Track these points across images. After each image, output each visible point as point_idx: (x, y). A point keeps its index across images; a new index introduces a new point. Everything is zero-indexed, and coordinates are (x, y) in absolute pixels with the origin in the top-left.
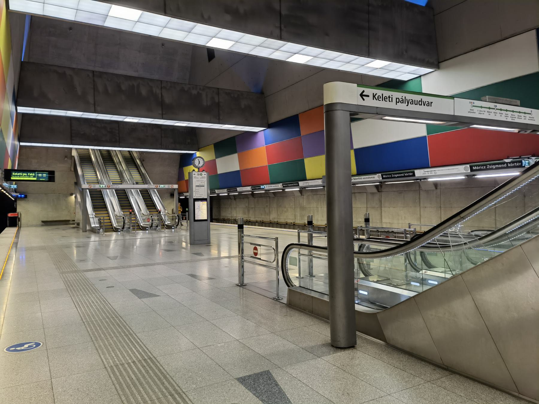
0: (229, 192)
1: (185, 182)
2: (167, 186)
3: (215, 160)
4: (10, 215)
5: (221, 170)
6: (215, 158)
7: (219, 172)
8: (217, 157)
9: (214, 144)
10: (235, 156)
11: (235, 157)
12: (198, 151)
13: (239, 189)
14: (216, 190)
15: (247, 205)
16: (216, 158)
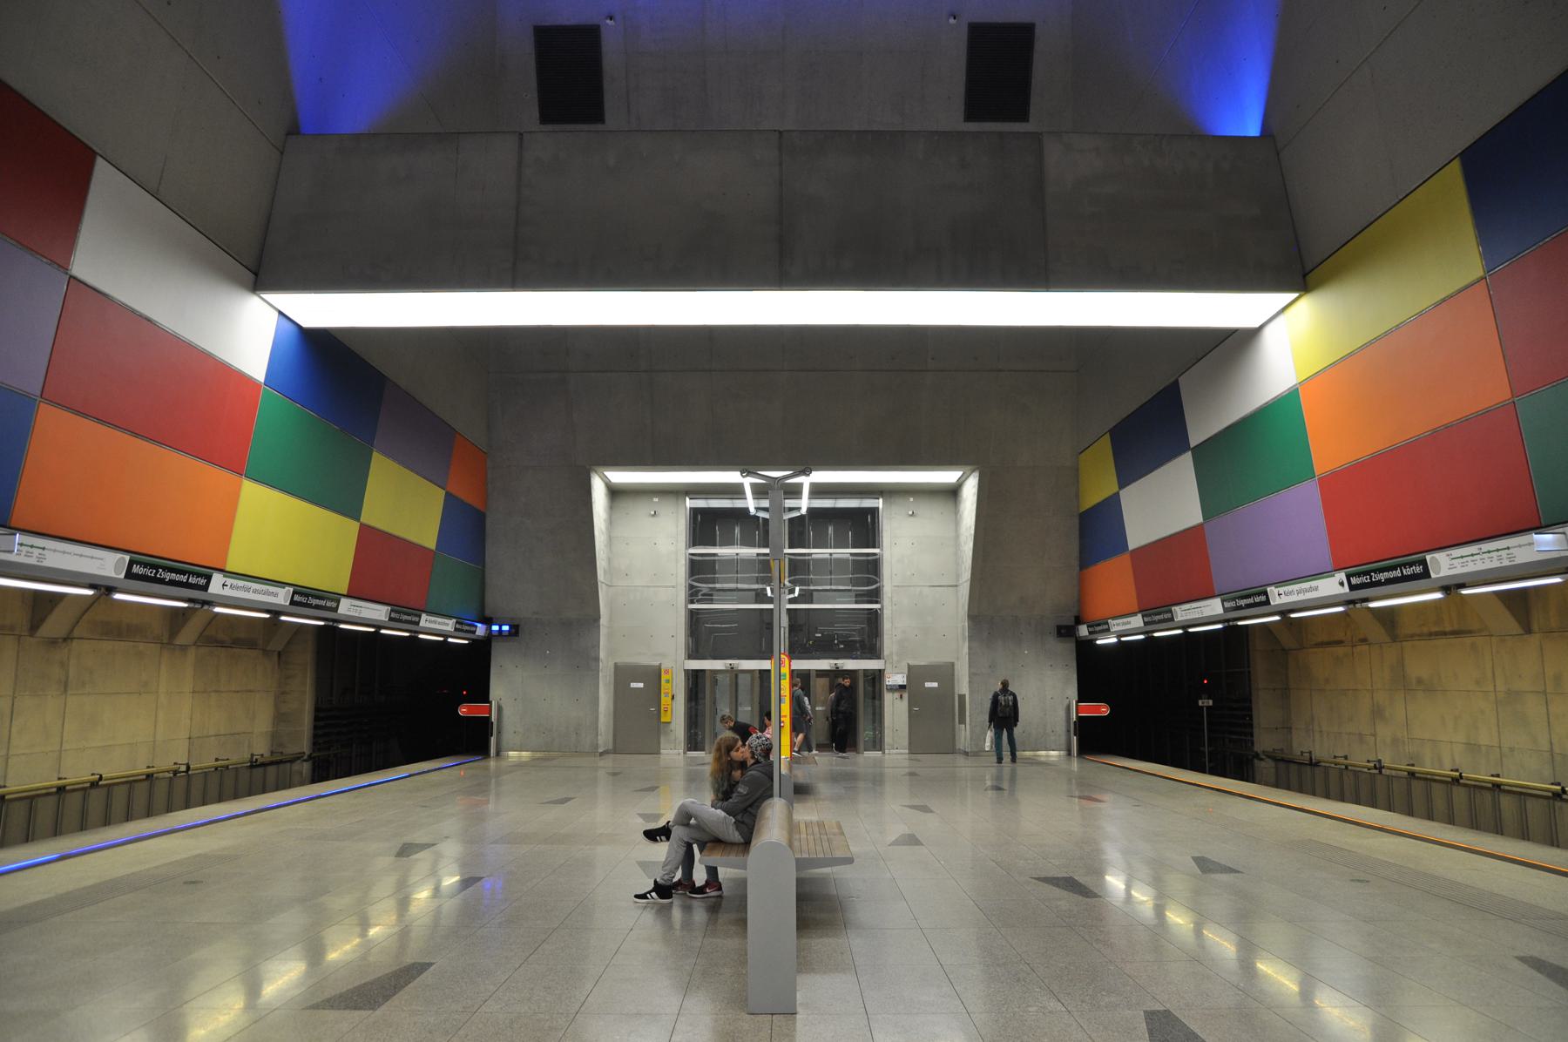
13: (1444, 564)
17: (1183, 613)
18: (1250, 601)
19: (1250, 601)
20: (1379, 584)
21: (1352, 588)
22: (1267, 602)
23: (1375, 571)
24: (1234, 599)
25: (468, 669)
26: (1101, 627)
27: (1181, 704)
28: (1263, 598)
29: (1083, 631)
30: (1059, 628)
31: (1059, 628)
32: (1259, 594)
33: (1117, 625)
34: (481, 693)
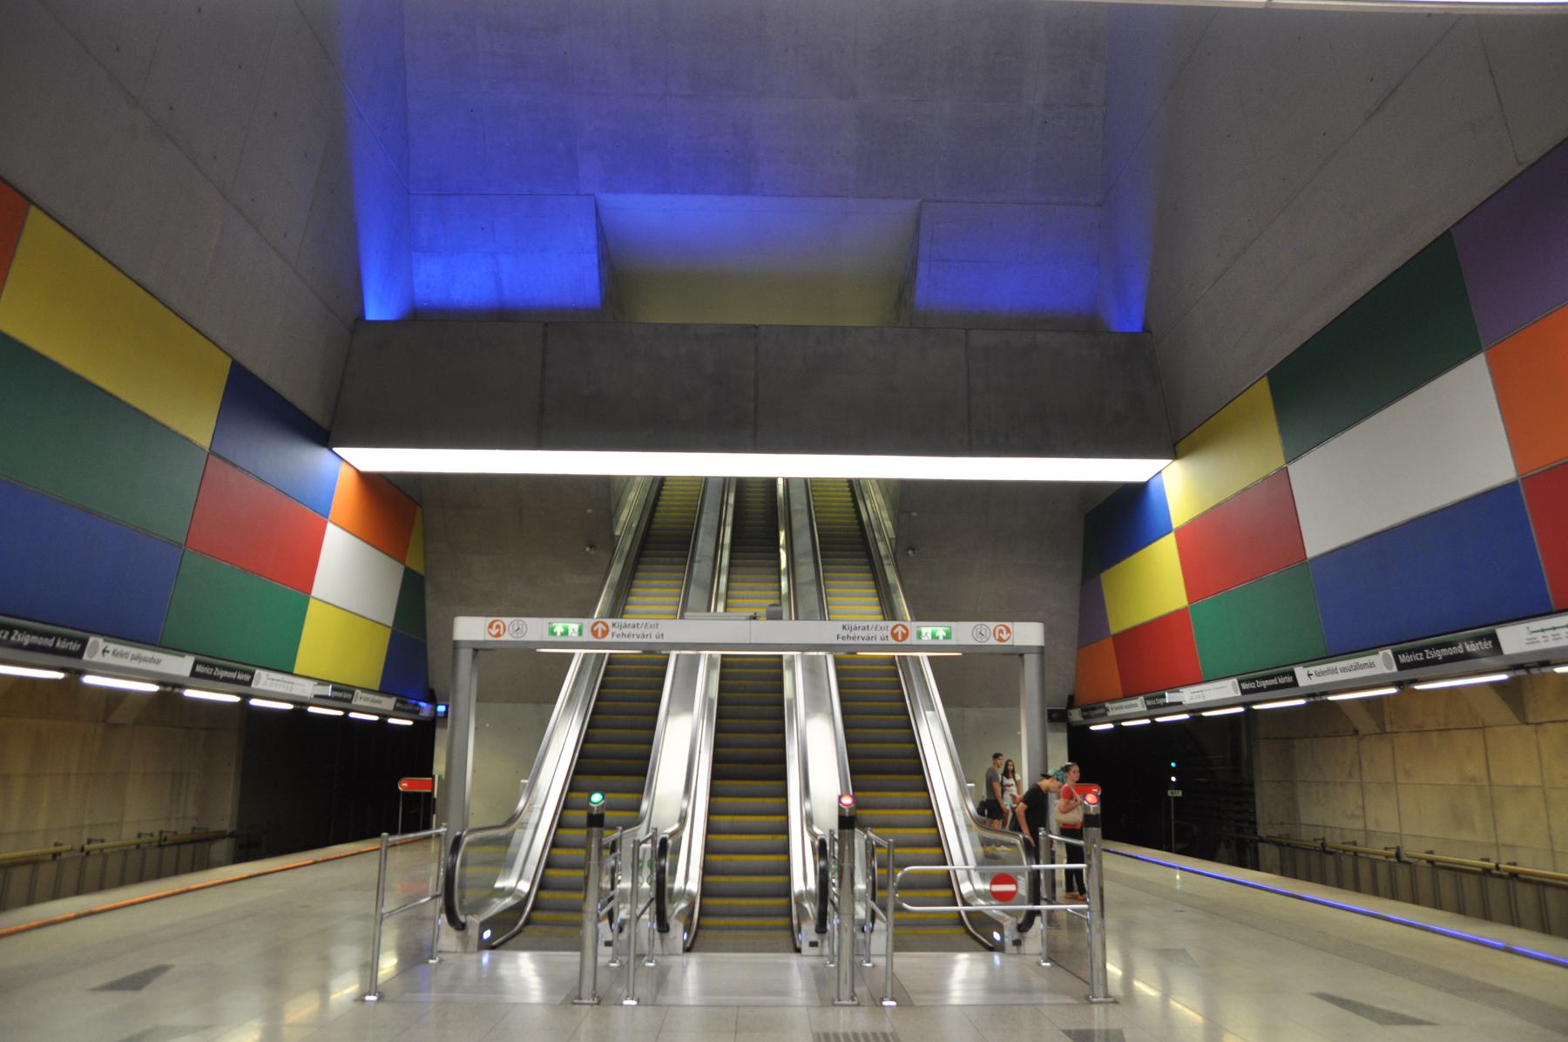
0: (1412, 666)
1: (1109, 646)
2: (965, 633)
3: (1284, 471)
4: (403, 786)
5: (1325, 528)
6: (1282, 463)
7: (1319, 539)
8: (1294, 453)
9: (1269, 374)
10: (1477, 369)
11: (1469, 388)
12: (1175, 455)
13: (1516, 639)
14: (1300, 672)
15: (1474, 768)
16: (1292, 457)
17: (1189, 696)
18: (1273, 682)
19: (1273, 682)
20: (1435, 662)
21: (1401, 667)
22: (1295, 684)
23: (1430, 647)
24: (1253, 680)
25: (416, 748)
26: (1094, 710)
27: (1179, 789)
28: (1289, 679)
29: (1076, 716)
30: (1050, 712)
31: (1050, 712)
32: (1284, 674)
33: (1115, 709)
34: (428, 772)
